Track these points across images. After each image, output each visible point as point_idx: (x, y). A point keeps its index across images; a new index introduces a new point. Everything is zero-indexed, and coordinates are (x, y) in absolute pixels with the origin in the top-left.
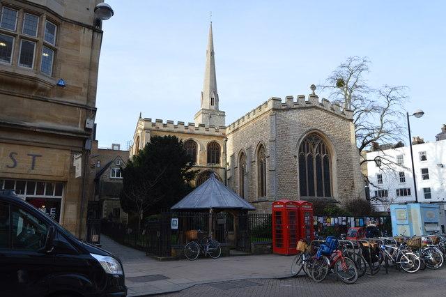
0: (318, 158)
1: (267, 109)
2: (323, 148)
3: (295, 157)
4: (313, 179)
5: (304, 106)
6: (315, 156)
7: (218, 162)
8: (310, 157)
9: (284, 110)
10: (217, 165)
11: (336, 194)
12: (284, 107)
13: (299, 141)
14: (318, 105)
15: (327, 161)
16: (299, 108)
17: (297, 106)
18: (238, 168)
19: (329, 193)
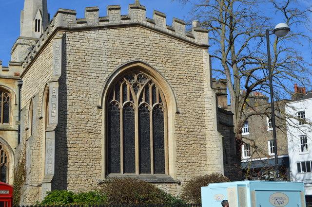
0: (142, 109)
1: (54, 29)
2: (151, 92)
4: (134, 145)
5: (117, 22)
6: (136, 106)
7: (6, 119)
10: (5, 125)
11: (172, 169)
12: (80, 26)
14: (145, 23)
15: (159, 114)
17: (106, 23)
18: (30, 130)
19: (160, 167)
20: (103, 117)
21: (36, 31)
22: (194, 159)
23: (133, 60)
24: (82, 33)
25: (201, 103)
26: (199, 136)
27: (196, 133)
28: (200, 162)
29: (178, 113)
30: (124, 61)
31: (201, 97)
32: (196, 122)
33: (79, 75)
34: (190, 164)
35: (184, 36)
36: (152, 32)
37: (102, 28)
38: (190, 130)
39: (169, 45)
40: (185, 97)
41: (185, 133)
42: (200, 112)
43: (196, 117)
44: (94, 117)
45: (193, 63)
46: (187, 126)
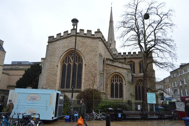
0: (75, 65)
3: (57, 66)
8: (69, 65)
9: (54, 41)
13: (61, 57)
15: (80, 67)
16: (63, 39)
24: (55, 43)
29: (85, 65)
30: (67, 49)
35: (90, 36)
37: (61, 39)
39: (84, 41)
41: (88, 73)
44: (55, 70)
45: (94, 45)
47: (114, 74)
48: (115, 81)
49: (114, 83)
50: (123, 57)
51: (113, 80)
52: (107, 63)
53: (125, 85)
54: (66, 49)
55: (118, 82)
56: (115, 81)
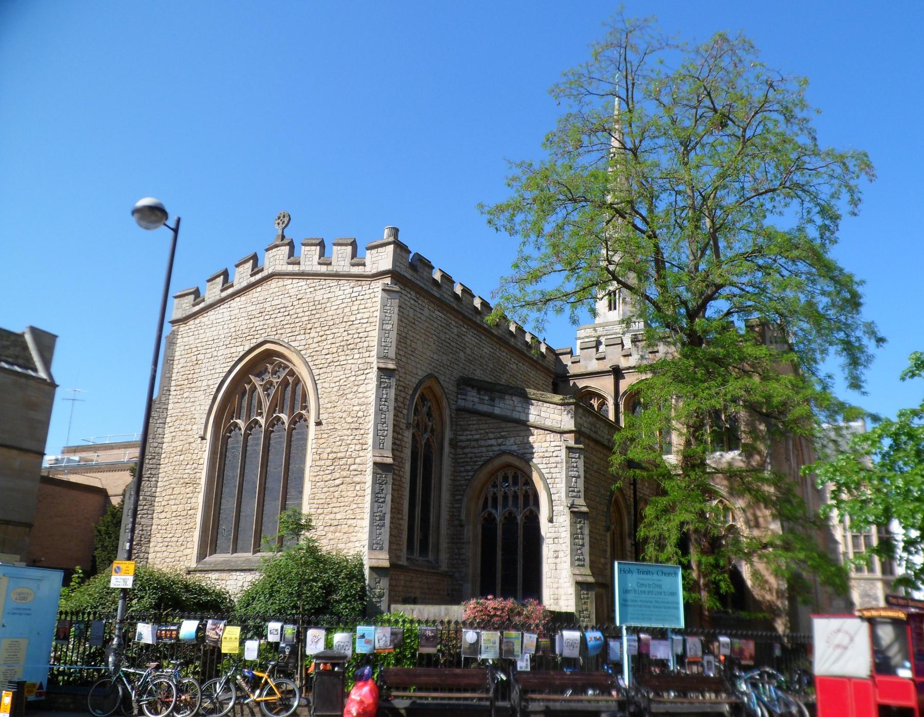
3: (203, 438)
20: (206, 455)
21: (610, 309)
22: (338, 516)
23: (254, 343)
24: (197, 321)
25: (366, 394)
26: (352, 467)
27: (350, 461)
28: (350, 522)
29: (319, 423)
30: (247, 348)
31: (366, 381)
32: (351, 437)
33: (187, 390)
34: (332, 528)
36: (295, 281)
37: (222, 301)
38: (339, 455)
39: (319, 295)
40: (335, 389)
42: (360, 414)
43: (353, 426)
44: (194, 457)
45: (359, 316)
46: (334, 450)
47: (497, 462)
48: (505, 505)
49: (499, 515)
50: (606, 365)
51: (495, 499)
52: (461, 403)
53: (551, 520)
54: (241, 350)
55: (495, 506)
56: (505, 505)
